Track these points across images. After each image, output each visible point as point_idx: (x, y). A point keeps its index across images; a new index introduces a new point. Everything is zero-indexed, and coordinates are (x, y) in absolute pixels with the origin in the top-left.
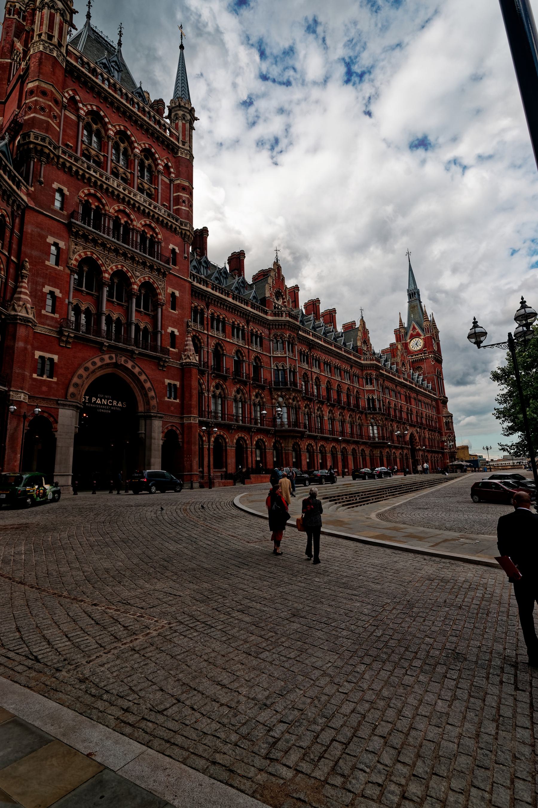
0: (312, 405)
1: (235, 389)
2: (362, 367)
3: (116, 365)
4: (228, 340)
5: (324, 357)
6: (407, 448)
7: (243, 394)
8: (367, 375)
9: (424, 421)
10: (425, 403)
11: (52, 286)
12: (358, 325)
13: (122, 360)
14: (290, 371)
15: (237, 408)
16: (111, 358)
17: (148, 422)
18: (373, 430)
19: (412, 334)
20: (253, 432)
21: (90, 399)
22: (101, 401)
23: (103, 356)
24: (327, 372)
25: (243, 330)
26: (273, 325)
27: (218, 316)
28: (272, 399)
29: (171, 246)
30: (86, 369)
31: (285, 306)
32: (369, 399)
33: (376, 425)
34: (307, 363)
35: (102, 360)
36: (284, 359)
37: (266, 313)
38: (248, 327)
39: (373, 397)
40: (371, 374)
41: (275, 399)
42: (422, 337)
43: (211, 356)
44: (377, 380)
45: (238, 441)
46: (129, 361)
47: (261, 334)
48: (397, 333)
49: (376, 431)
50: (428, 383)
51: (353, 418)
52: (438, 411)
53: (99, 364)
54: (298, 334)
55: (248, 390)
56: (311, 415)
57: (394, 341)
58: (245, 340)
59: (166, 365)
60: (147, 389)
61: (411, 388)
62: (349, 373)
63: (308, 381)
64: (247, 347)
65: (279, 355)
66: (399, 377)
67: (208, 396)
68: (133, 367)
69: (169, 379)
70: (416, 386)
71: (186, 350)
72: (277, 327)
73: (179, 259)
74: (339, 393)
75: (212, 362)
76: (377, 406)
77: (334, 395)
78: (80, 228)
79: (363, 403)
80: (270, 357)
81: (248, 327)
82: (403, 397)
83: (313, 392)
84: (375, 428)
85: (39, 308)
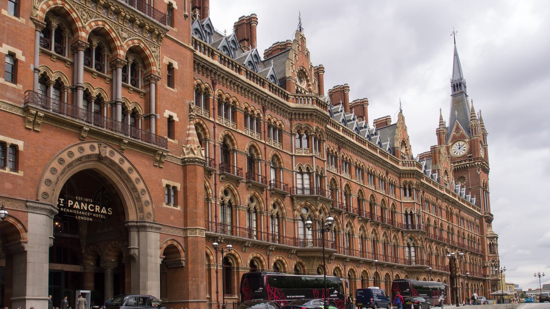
0: (341, 219)
1: (249, 196)
2: (401, 174)
3: (100, 158)
4: (240, 131)
5: (355, 159)
6: (446, 275)
7: (259, 203)
8: (405, 183)
9: (466, 243)
10: (467, 221)
12: (394, 120)
13: (107, 152)
14: (317, 175)
15: (250, 220)
16: (92, 148)
18: (410, 252)
19: (454, 136)
20: (270, 250)
21: (66, 203)
23: (82, 145)
24: (359, 178)
25: (258, 120)
26: (295, 114)
28: (294, 210)
30: (61, 161)
31: (310, 91)
32: (406, 214)
33: (414, 246)
34: (336, 166)
35: (82, 149)
36: (310, 159)
37: (287, 98)
38: (264, 115)
39: (411, 212)
40: (411, 183)
41: (297, 210)
42: (467, 140)
43: (219, 151)
44: (418, 191)
45: (252, 262)
46: (115, 153)
47: (280, 125)
48: (439, 133)
49: (413, 254)
50: (472, 197)
51: (387, 237)
52: (482, 232)
53: (77, 155)
54: (326, 127)
55: (264, 198)
56: (339, 231)
57: (435, 143)
58: (261, 133)
59: (163, 160)
61: (454, 203)
62: (385, 181)
63: (337, 190)
64: (263, 142)
65: (303, 154)
66: (441, 188)
67: (216, 204)
68: (122, 161)
69: (168, 179)
70: (459, 199)
71: (187, 142)
72: (301, 117)
74: (372, 205)
75: (219, 160)
76: (417, 223)
77: (366, 208)
79: (400, 219)
80: (292, 156)
81: (264, 115)
82: (444, 213)
83: (342, 204)
84: (412, 249)
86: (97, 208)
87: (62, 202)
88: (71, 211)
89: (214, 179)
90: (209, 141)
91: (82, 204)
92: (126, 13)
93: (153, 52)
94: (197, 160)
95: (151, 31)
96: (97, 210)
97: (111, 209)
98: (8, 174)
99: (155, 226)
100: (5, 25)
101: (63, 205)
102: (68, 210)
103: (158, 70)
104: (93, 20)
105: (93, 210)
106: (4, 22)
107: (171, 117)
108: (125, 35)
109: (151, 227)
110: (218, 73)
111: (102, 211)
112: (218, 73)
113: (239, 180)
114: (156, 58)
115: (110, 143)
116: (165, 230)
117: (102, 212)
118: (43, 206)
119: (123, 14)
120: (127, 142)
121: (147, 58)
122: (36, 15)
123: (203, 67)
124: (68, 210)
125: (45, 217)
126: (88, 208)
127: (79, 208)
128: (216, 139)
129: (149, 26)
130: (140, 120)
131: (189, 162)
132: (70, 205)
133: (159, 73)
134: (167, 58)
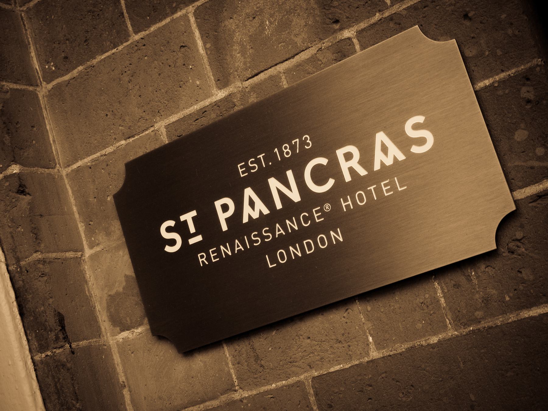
22: (267, 199)
87: (192, 230)
91: (274, 184)
96: (351, 170)
101: (199, 238)
102: (226, 250)
105: (331, 182)
111: (379, 160)
117: (377, 167)
124: (226, 250)
127: (266, 211)
132: (227, 220)
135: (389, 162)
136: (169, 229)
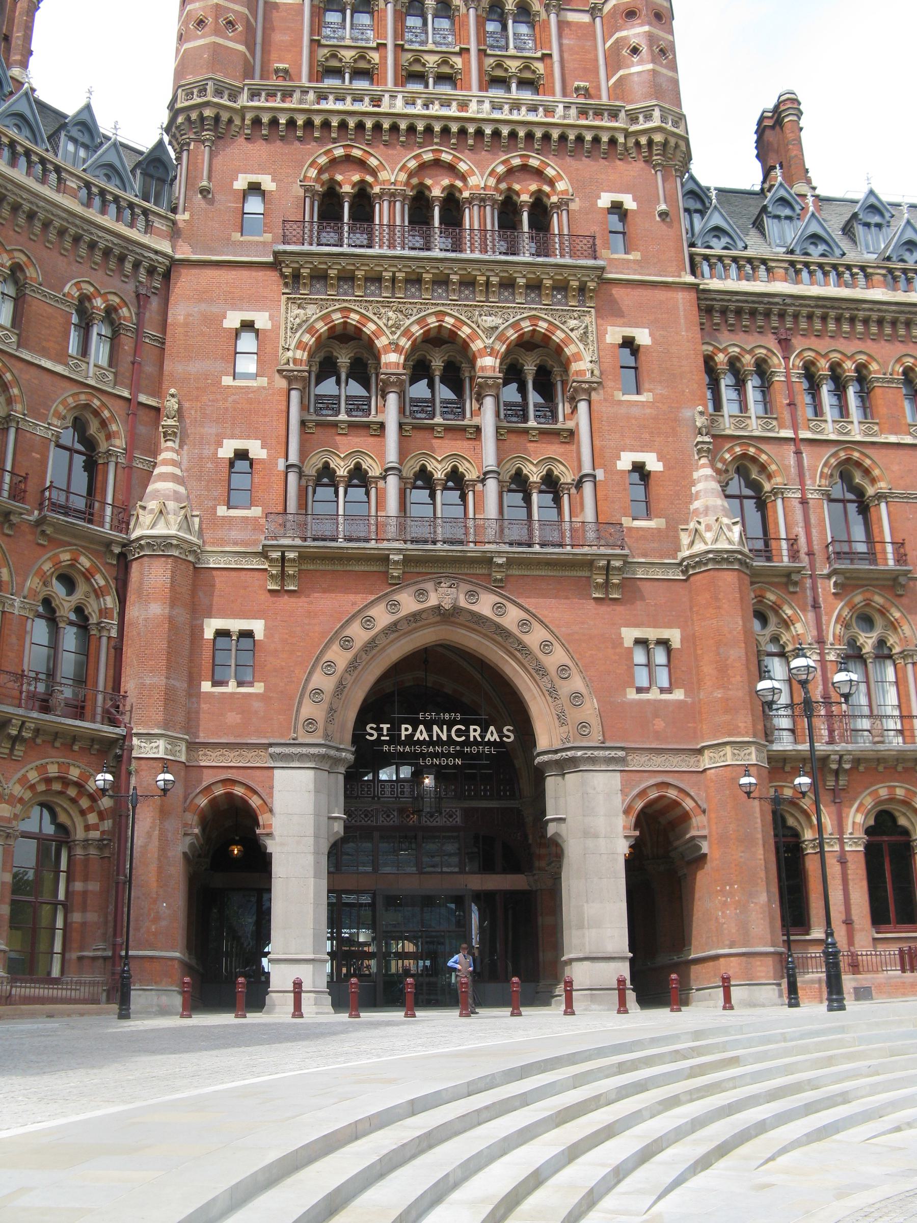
4: (893, 439)
11: (241, 438)
17: (571, 779)
27: (835, 368)
29: (605, 200)
60: (552, 670)
73: (638, 226)
78: (301, 260)
85: (211, 504)
86: (475, 732)
87: (385, 733)
88: (407, 749)
89: (809, 593)
90: (782, 493)
91: (435, 728)
92: (488, 274)
93: (572, 330)
94: (740, 557)
95: (562, 287)
96: (474, 736)
97: (511, 728)
98: (232, 694)
99: (601, 753)
100: (228, 405)
101: (387, 738)
102: (400, 748)
103: (590, 366)
104: (413, 319)
105: (464, 738)
106: (225, 400)
107: (639, 468)
108: (490, 321)
109: (593, 760)
110: (790, 310)
111: (488, 736)
112: (790, 310)
113: (897, 577)
114: (581, 341)
115: (466, 574)
116: (637, 762)
117: (486, 740)
118: (304, 750)
119: (481, 279)
120: (505, 559)
121: (559, 350)
122: (285, 361)
123: (724, 312)
124: (400, 748)
125: (311, 773)
126: (449, 736)
127: (427, 739)
128: (808, 482)
129: (552, 278)
130: (566, 497)
131: (694, 567)
133: (592, 372)
134: (617, 329)
135: (492, 739)
136: (372, 728)
